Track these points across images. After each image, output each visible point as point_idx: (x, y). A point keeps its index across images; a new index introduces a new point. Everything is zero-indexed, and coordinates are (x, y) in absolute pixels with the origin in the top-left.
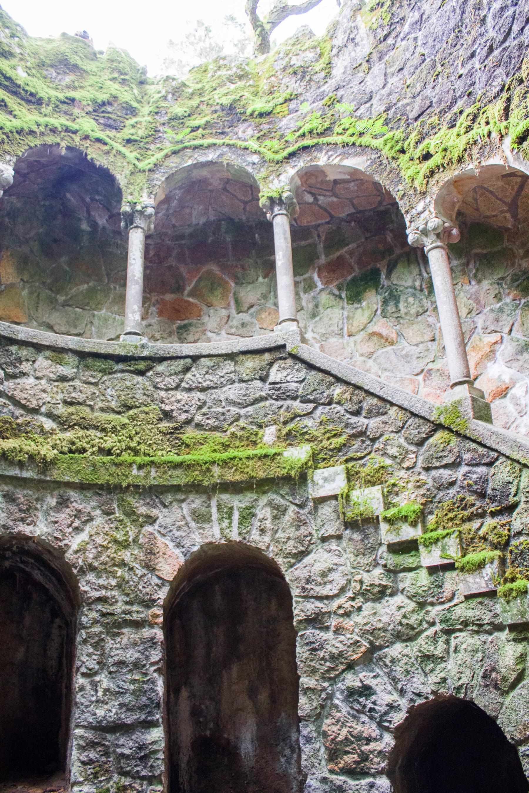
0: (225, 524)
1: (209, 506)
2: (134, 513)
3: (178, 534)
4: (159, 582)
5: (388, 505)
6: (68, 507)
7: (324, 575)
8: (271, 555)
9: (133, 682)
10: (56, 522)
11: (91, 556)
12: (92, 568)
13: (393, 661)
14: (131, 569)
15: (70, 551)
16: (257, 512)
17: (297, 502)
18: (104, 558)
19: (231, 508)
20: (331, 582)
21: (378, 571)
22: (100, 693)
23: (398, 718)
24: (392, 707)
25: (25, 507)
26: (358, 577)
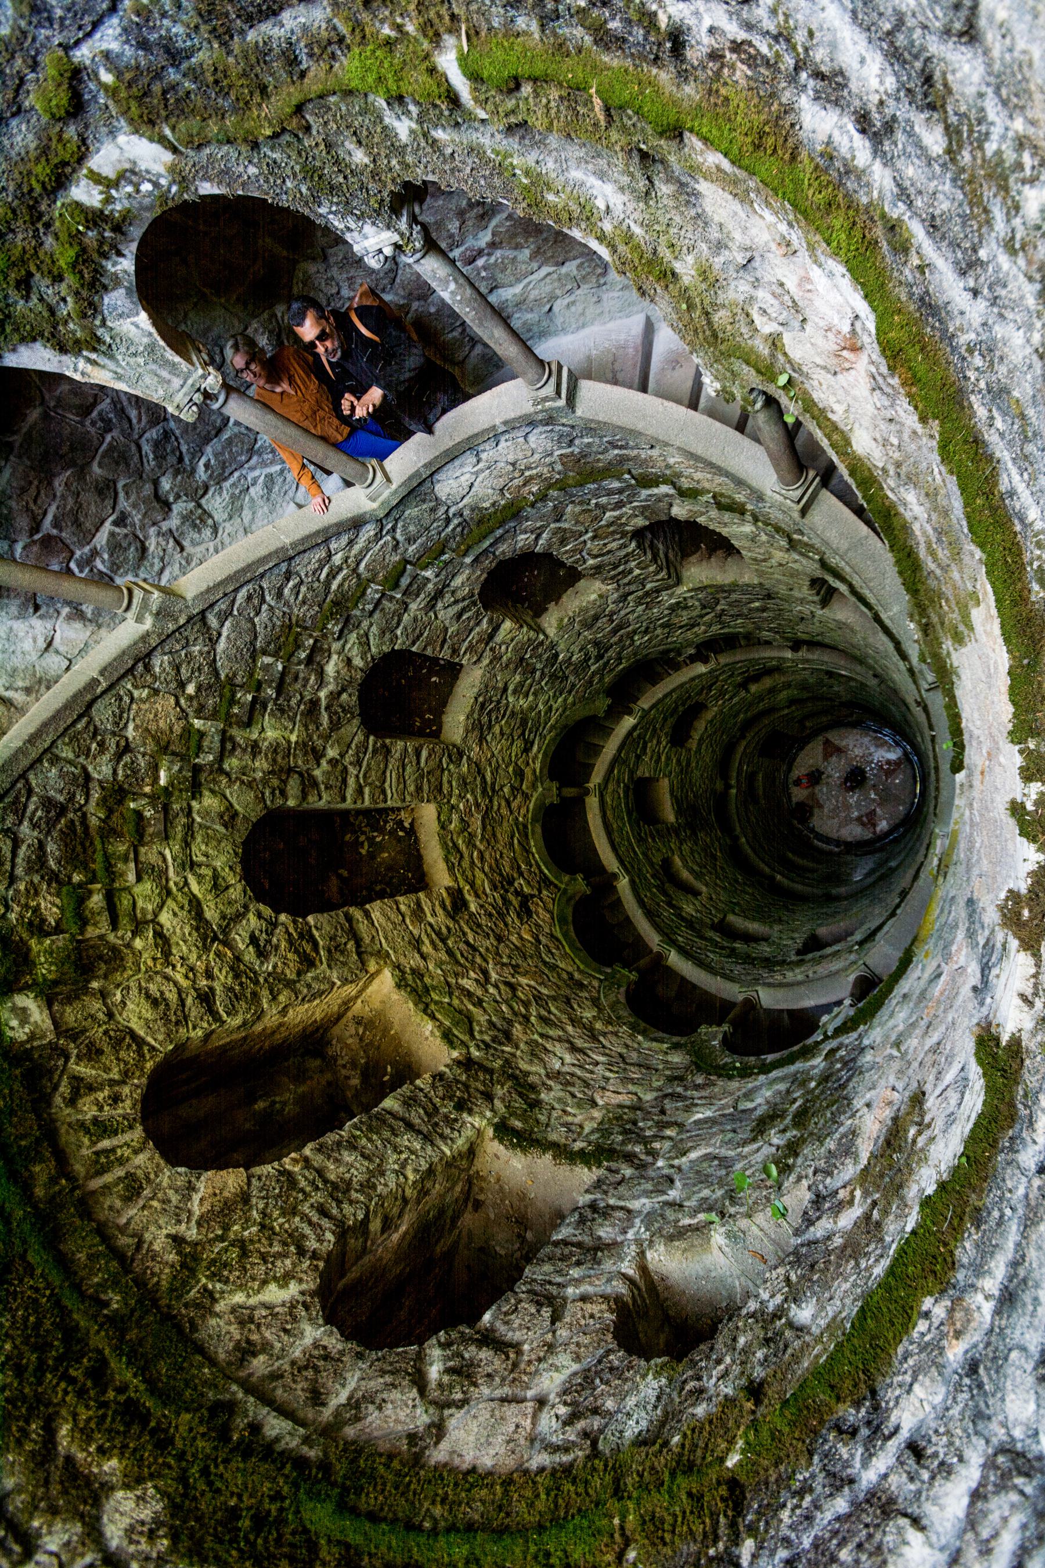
0: (127, 1152)
1: (106, 1187)
2: (183, 1265)
3: (175, 1198)
4: (254, 1181)
5: (58, 930)
6: (248, 1341)
7: (155, 1003)
8: (144, 1080)
9: (370, 1140)
10: (286, 1331)
11: (288, 1262)
12: (301, 1252)
13: (223, 917)
14: (264, 1214)
15: (304, 1286)
16: (89, 1116)
17: (61, 1062)
18: (277, 1248)
19: (97, 1153)
20: (162, 993)
21: (138, 943)
22: (403, 1156)
23: (267, 911)
24: (259, 916)
25: (310, 1373)
26: (150, 963)
